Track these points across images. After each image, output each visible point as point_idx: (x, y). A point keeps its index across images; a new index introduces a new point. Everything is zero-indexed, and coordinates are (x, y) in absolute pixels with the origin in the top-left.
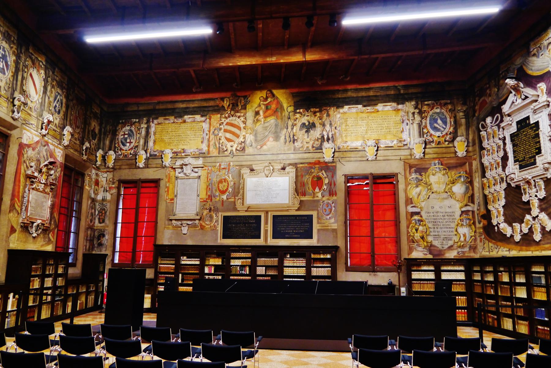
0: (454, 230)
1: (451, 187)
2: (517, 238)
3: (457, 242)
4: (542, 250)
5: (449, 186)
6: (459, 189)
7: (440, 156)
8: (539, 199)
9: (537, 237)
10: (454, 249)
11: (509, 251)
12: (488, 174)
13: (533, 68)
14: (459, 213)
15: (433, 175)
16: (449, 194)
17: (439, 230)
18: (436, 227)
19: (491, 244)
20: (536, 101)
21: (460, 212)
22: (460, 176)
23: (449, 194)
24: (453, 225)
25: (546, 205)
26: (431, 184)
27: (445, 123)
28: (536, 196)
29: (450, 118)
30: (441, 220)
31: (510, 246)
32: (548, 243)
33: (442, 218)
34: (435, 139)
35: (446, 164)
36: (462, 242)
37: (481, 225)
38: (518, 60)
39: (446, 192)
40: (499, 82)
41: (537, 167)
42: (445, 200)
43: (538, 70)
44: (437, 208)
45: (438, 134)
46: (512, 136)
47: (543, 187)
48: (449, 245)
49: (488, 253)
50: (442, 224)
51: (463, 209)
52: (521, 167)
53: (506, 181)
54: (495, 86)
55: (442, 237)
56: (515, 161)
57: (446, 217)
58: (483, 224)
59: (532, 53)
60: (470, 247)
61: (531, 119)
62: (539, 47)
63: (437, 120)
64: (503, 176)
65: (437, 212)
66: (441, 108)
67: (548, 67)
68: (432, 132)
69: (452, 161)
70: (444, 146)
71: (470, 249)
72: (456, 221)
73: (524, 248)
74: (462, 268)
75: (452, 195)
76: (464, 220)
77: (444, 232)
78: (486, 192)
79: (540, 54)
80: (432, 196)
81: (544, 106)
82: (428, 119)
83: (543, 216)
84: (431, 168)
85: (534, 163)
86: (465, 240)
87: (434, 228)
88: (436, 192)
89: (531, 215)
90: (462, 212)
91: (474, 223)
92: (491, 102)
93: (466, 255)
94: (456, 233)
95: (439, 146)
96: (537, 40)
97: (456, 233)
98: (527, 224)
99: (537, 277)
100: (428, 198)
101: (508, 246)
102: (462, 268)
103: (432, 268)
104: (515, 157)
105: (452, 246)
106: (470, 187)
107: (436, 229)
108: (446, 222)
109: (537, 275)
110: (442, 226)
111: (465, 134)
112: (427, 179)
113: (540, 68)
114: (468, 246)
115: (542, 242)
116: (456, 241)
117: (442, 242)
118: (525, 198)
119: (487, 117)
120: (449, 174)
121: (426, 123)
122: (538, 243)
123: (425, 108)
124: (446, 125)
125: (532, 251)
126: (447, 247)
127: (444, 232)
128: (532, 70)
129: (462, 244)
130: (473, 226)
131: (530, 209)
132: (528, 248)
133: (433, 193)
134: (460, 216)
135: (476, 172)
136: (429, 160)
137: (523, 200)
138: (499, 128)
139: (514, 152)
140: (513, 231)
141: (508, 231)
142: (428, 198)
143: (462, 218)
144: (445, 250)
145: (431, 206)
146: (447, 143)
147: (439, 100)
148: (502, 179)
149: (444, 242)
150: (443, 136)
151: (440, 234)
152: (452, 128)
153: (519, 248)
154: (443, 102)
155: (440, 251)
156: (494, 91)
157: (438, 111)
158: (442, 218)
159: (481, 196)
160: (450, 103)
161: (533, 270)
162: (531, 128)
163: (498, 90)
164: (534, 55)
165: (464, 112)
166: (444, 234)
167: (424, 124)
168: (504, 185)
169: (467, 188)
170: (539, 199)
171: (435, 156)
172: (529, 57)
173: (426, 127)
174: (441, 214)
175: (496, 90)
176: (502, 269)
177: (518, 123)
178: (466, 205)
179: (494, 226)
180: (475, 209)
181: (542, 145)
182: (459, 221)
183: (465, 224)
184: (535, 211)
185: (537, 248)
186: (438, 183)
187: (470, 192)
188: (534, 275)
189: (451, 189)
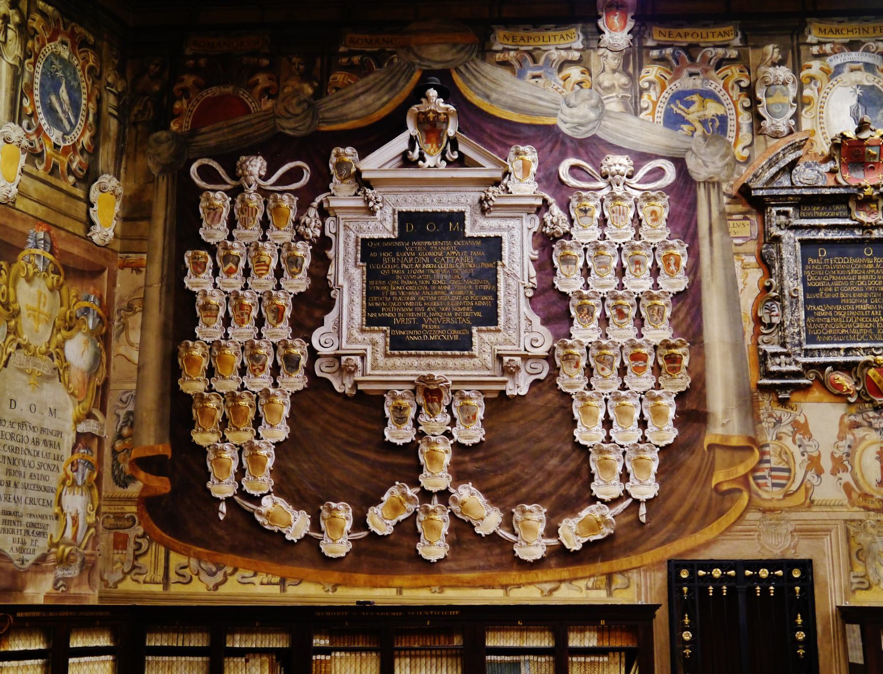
0: (53, 497)
1: (64, 340)
2: (337, 545)
3: (57, 545)
4: (442, 588)
5: (59, 336)
6: (78, 351)
7: (53, 218)
8: (458, 448)
9: (434, 548)
10: (43, 572)
11: (282, 582)
12: (209, 331)
13: (494, 96)
14: (69, 439)
15: (29, 280)
16: (56, 363)
17: (20, 492)
18: (13, 479)
19: (176, 559)
20: (497, 183)
21: (73, 436)
22: (87, 309)
23: (56, 363)
24: (54, 480)
25: (481, 464)
26: (19, 312)
27: (75, 105)
28: (448, 435)
29: (89, 99)
30: (28, 458)
31: (287, 570)
32: (473, 569)
33: (31, 447)
34: (48, 150)
35: (64, 253)
36: (69, 545)
37: (134, 489)
38: (435, 49)
39: (51, 356)
40: (327, 71)
41: (472, 356)
42: (45, 385)
43: (513, 108)
44: (22, 411)
45: (55, 135)
46: (370, 250)
47: (480, 414)
48: (38, 553)
49: (158, 588)
50: (29, 471)
51: (82, 428)
52: (398, 344)
53: (309, 371)
54: (306, 77)
55: (26, 520)
56: (370, 322)
57: (41, 448)
58: (145, 488)
59: (499, 57)
60: (83, 562)
61: (467, 223)
62: (529, 52)
63: (60, 85)
64: (299, 349)
65: (22, 424)
66: (73, 52)
67: (555, 115)
68: (43, 120)
69: (75, 250)
70: (64, 186)
71: (81, 572)
72: (62, 465)
73: (362, 577)
74: (104, 641)
75: (62, 370)
76: (80, 467)
77: (32, 501)
78: (193, 385)
79: (529, 73)
80: (19, 358)
81: (531, 206)
82: (40, 68)
83: (468, 494)
84: (26, 252)
85: (465, 344)
86: (75, 537)
87: (8, 484)
88: (27, 347)
89: (416, 483)
90: (79, 436)
91: (98, 481)
92: (272, 115)
93: (72, 591)
94: (57, 510)
95: (52, 180)
96: (522, 33)
97: (57, 510)
98: (396, 509)
99: (509, 663)
100: (5, 365)
101: (277, 568)
102: (104, 641)
103: (36, 644)
104: (369, 309)
105: (43, 558)
106: (104, 355)
107: (12, 489)
108: (41, 465)
109: (499, 658)
110: (28, 481)
111: (112, 169)
112: (11, 290)
113: (521, 105)
114: (79, 560)
115: (446, 565)
116: (55, 540)
117: (24, 543)
118: (398, 434)
119: (253, 152)
120: (64, 290)
121: (32, 76)
122: (427, 566)
123: (36, 23)
124: (76, 117)
125: (400, 590)
126: (31, 558)
127: (32, 501)
128: (488, 97)
129: (67, 550)
130: (95, 492)
131: (420, 469)
132: (379, 579)
133: (19, 347)
134: (73, 453)
135: (130, 308)
136: (24, 221)
137: (388, 437)
138: (303, 208)
139: (370, 293)
140: (316, 525)
141: (297, 525)
142: (5, 365)
143: (76, 456)
144: (27, 571)
145: (9, 395)
146: (71, 179)
147: (72, 19)
148: (292, 363)
149: (28, 540)
150: (66, 151)
151: (21, 508)
152: (88, 134)
153: (336, 576)
154: (79, 30)
155: (15, 575)
156: (297, 92)
157: (66, 54)
158: (31, 447)
159: (151, 395)
160: (93, 47)
161: (490, 643)
162: (459, 249)
163: (320, 93)
164: (505, 64)
165: (118, 96)
166: (31, 508)
167: (26, 79)
168: (297, 381)
169: (97, 358)
170: (458, 448)
171: (40, 211)
172: (484, 59)
173: (30, 89)
174: (31, 435)
175: (310, 91)
176: (320, 642)
177: (405, 218)
178: (89, 416)
179: (219, 501)
180: (108, 435)
181: (501, 303)
182: (69, 473)
183: (80, 483)
184: (436, 478)
185: (423, 579)
186: (35, 313)
187: (102, 374)
188: (488, 658)
189: (63, 349)
